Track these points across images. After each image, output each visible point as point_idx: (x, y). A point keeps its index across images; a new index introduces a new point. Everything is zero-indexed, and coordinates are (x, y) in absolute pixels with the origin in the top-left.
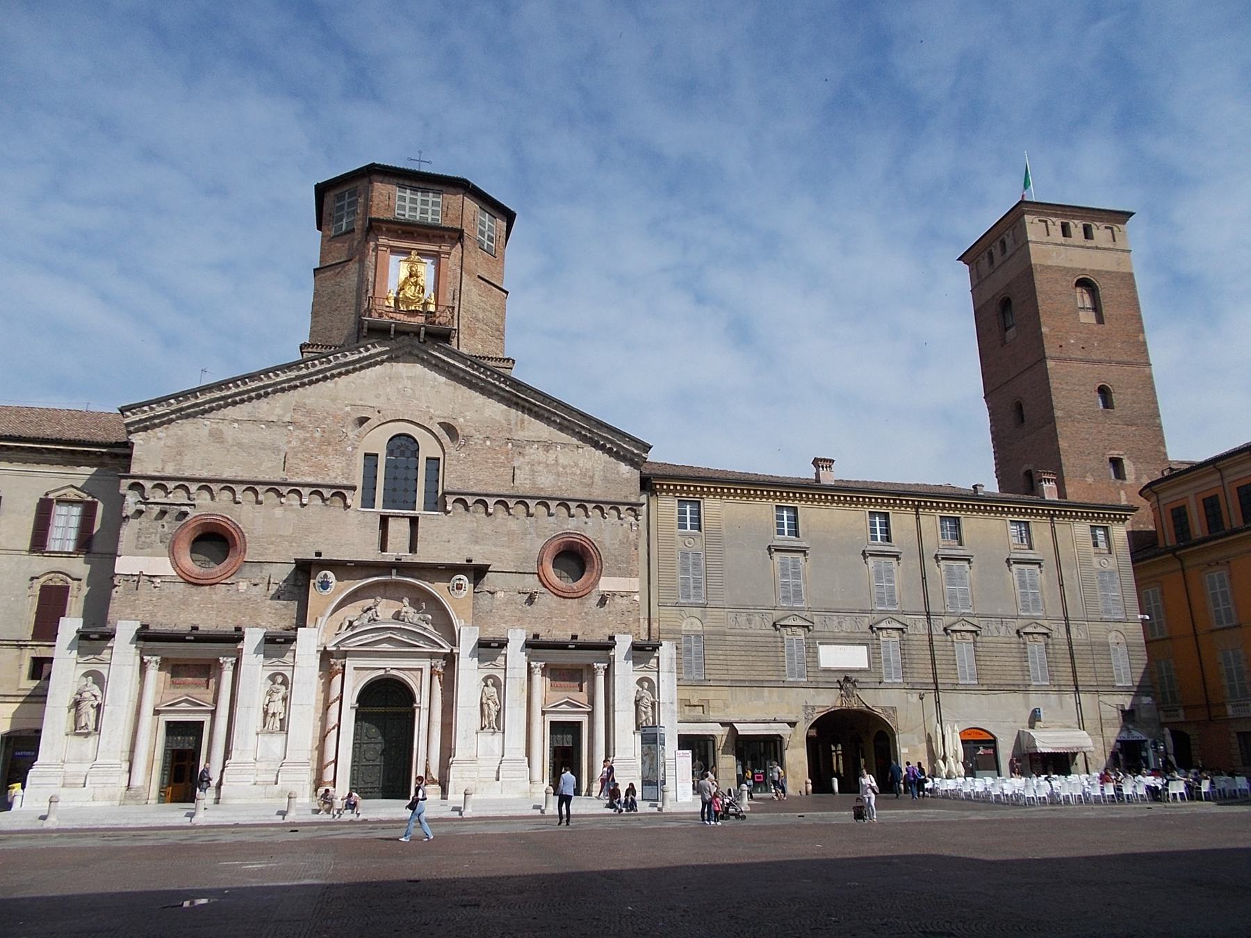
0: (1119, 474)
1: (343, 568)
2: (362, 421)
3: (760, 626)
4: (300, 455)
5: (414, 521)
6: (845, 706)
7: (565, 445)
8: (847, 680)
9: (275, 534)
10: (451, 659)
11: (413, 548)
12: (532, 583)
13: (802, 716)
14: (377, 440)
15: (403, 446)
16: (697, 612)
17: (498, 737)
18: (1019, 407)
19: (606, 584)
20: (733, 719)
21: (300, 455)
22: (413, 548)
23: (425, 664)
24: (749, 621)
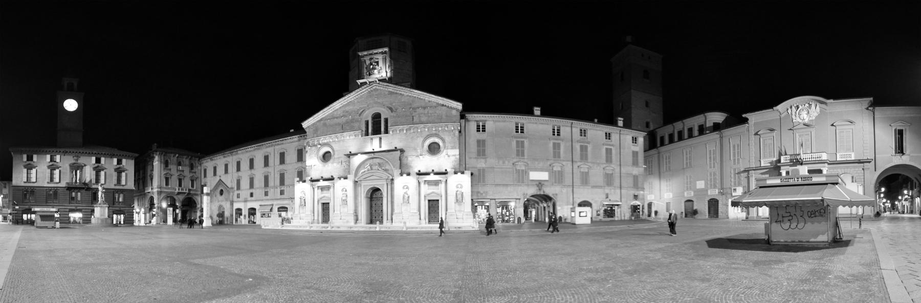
8: (540, 184)
13: (522, 198)
16: (483, 160)
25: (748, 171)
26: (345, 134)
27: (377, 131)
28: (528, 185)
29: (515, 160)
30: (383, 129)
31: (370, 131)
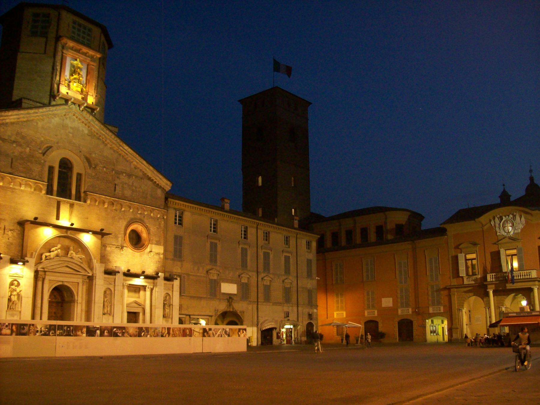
4: (19, 161)
6: (228, 310)
7: (136, 177)
8: (230, 298)
10: (91, 279)
15: (66, 165)
16: (179, 263)
17: (111, 317)
20: (190, 314)
21: (19, 161)
24: (198, 269)
25: (449, 289)
26: (19, 179)
27: (64, 191)
28: (220, 299)
29: (209, 267)
30: (74, 192)
31: (55, 187)
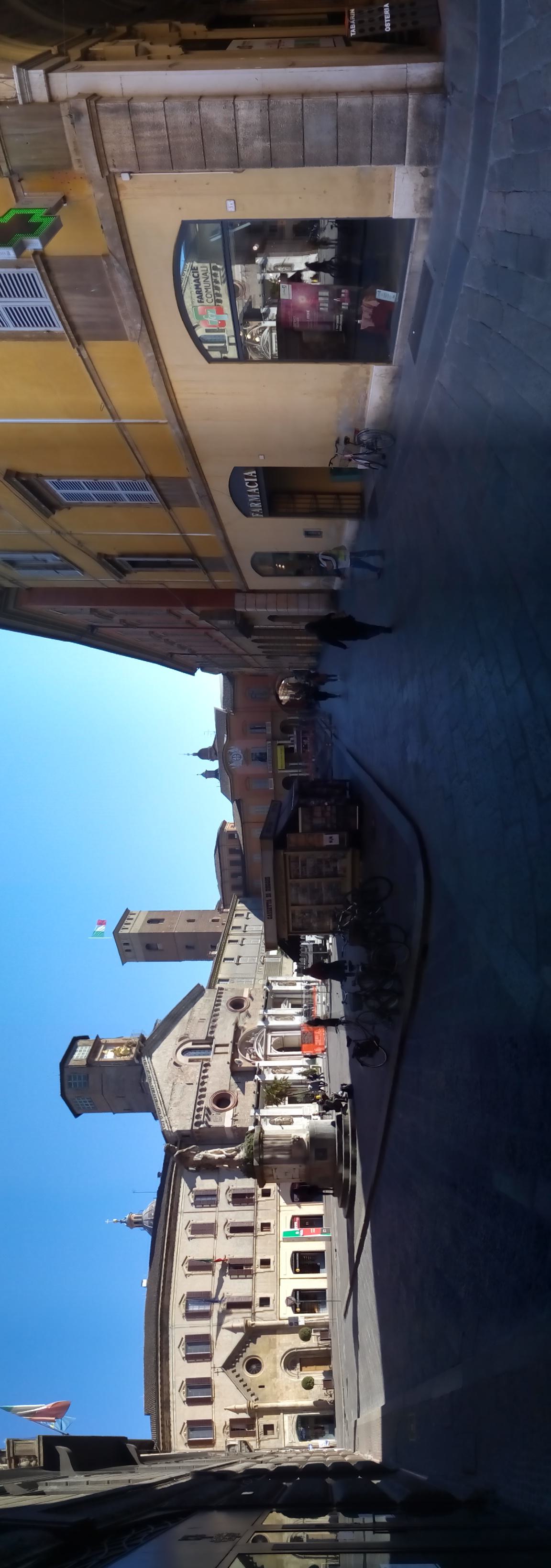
0: (217, 921)
1: (234, 1055)
2: (175, 1064)
3: (262, 967)
5: (217, 1046)
9: (219, 1077)
11: (227, 1045)
12: (243, 1014)
14: (183, 1059)
18: (187, 947)
19: (246, 995)
22: (227, 1045)
23: (269, 1036)
